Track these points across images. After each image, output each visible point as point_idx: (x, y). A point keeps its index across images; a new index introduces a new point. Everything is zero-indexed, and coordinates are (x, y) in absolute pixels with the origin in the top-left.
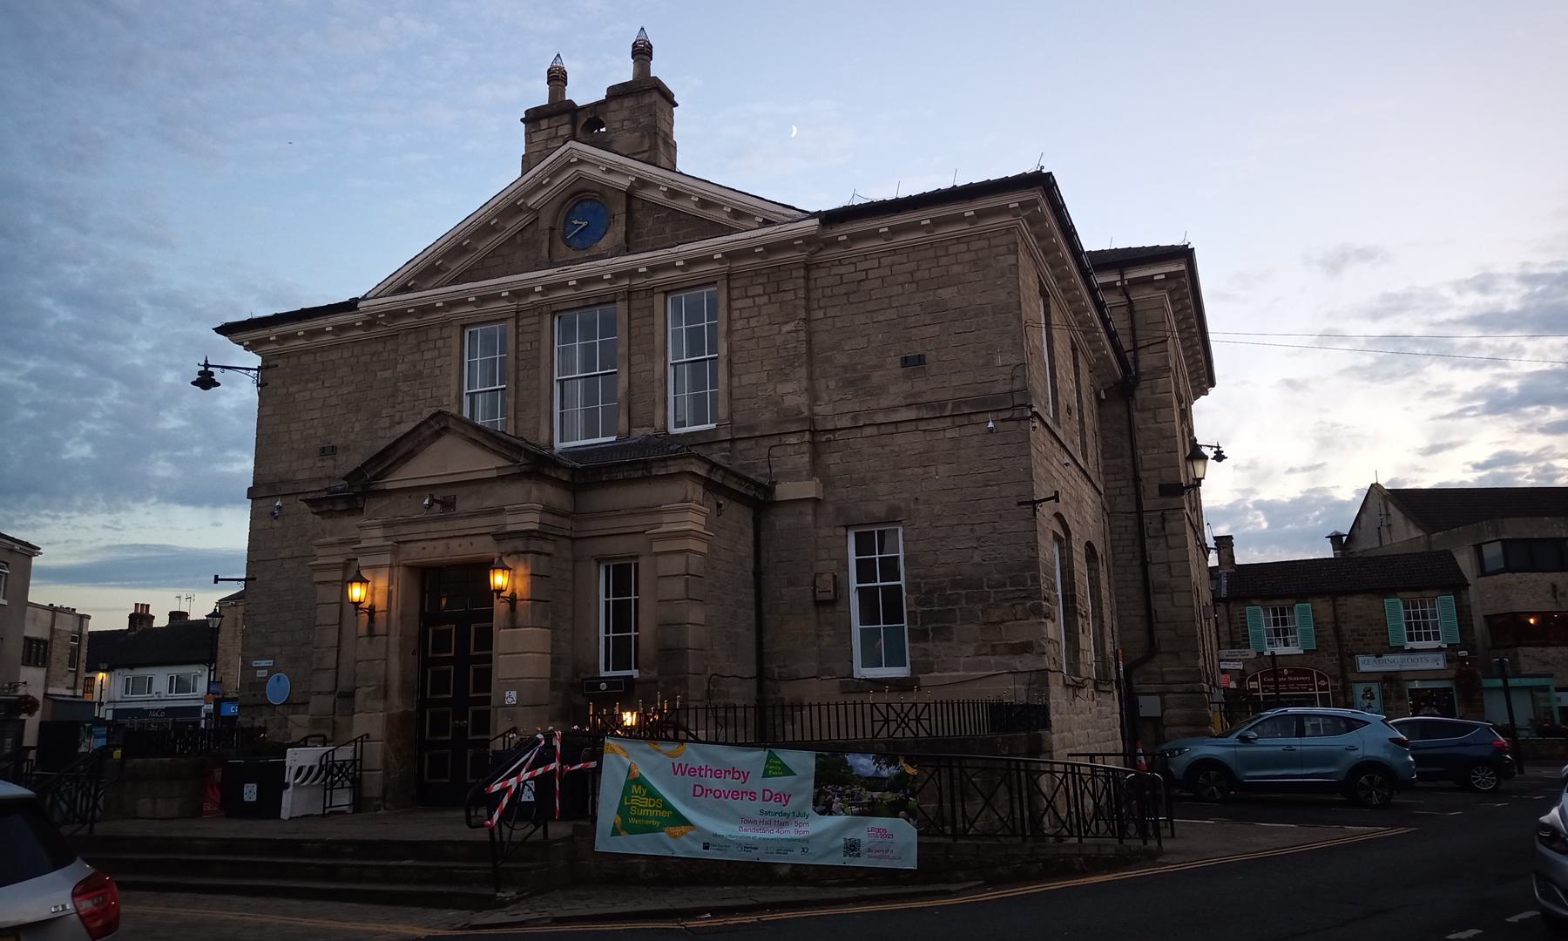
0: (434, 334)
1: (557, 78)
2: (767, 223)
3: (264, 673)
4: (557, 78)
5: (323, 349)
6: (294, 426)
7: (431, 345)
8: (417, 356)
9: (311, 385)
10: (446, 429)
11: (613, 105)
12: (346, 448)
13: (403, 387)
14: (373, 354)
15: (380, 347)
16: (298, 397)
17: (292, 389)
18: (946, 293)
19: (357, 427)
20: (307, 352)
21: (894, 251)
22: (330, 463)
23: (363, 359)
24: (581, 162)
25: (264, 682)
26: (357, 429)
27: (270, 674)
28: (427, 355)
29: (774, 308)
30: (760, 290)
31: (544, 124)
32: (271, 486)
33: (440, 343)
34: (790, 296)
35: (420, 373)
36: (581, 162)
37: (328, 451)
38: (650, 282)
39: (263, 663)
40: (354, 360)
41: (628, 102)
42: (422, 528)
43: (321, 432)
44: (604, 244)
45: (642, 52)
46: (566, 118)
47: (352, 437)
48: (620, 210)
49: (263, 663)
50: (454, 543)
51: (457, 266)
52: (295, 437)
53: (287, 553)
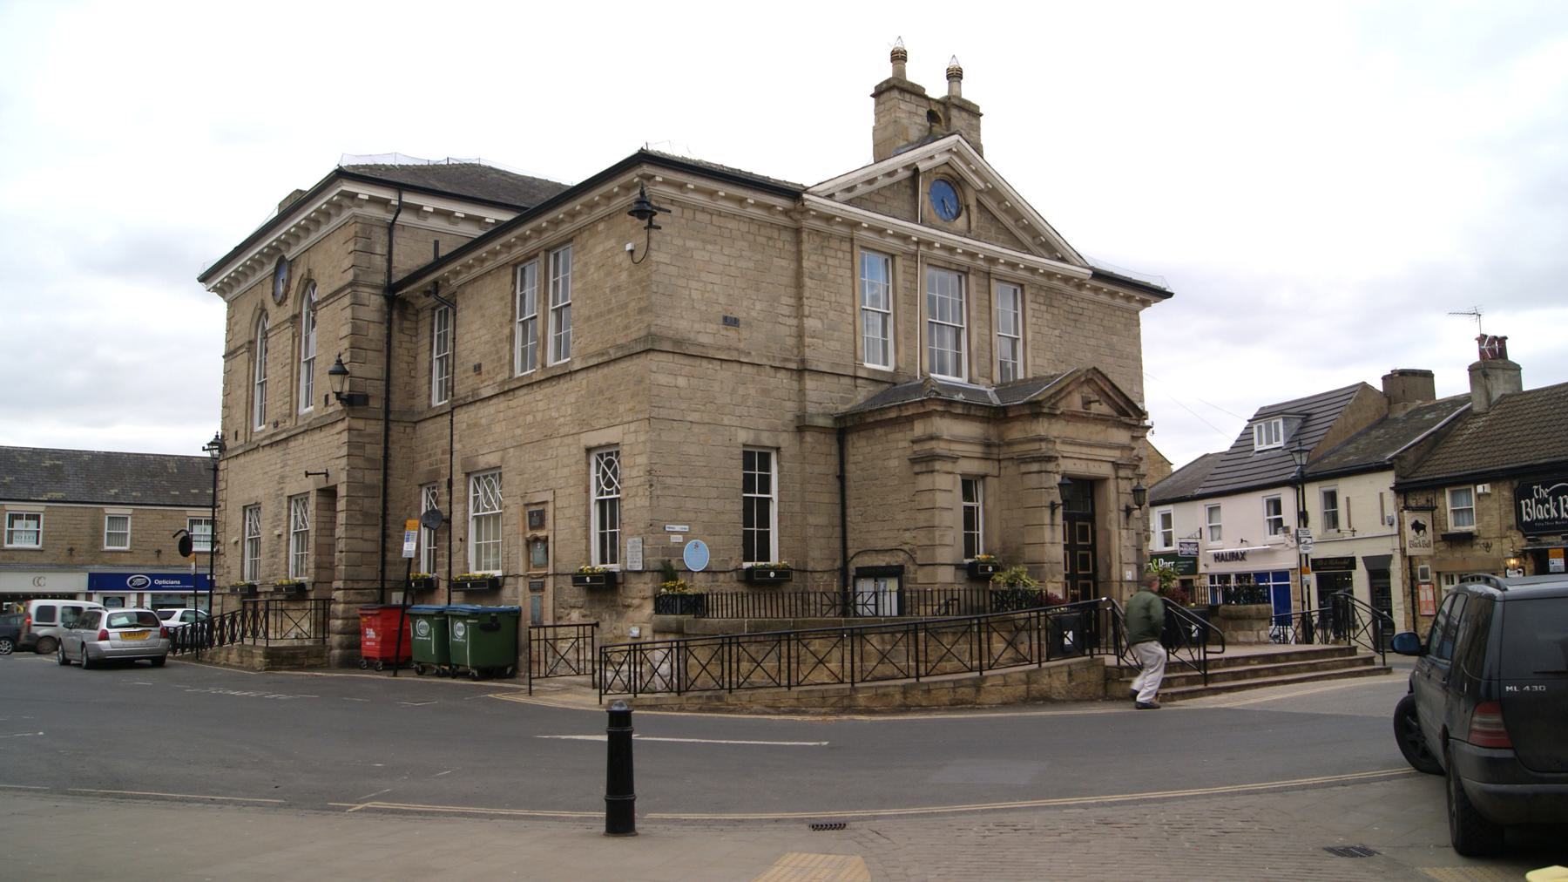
0: (834, 244)
1: (899, 57)
2: (1063, 260)
3: (680, 538)
4: (899, 57)
5: (720, 214)
6: (693, 284)
7: (832, 253)
8: (821, 259)
9: (709, 247)
10: (1089, 381)
11: (954, 113)
12: (749, 325)
13: (808, 282)
14: (770, 238)
15: (775, 235)
16: (698, 255)
17: (690, 244)
18: (1115, 338)
19: (758, 306)
20: (703, 210)
21: (1094, 302)
22: (731, 333)
23: (761, 240)
24: (958, 154)
25: (679, 549)
26: (758, 306)
27: (685, 542)
28: (830, 261)
29: (1048, 316)
30: (1041, 300)
31: (907, 96)
32: (677, 342)
33: (840, 254)
34: (1056, 311)
35: (823, 278)
36: (958, 154)
37: (731, 322)
38: (993, 269)
39: (678, 528)
40: (751, 237)
41: (964, 114)
42: (1077, 449)
43: (722, 300)
44: (961, 222)
45: (955, 75)
46: (925, 103)
47: (754, 314)
48: (972, 203)
49: (678, 528)
50: (1091, 464)
51: (862, 190)
52: (696, 295)
53: (695, 417)
